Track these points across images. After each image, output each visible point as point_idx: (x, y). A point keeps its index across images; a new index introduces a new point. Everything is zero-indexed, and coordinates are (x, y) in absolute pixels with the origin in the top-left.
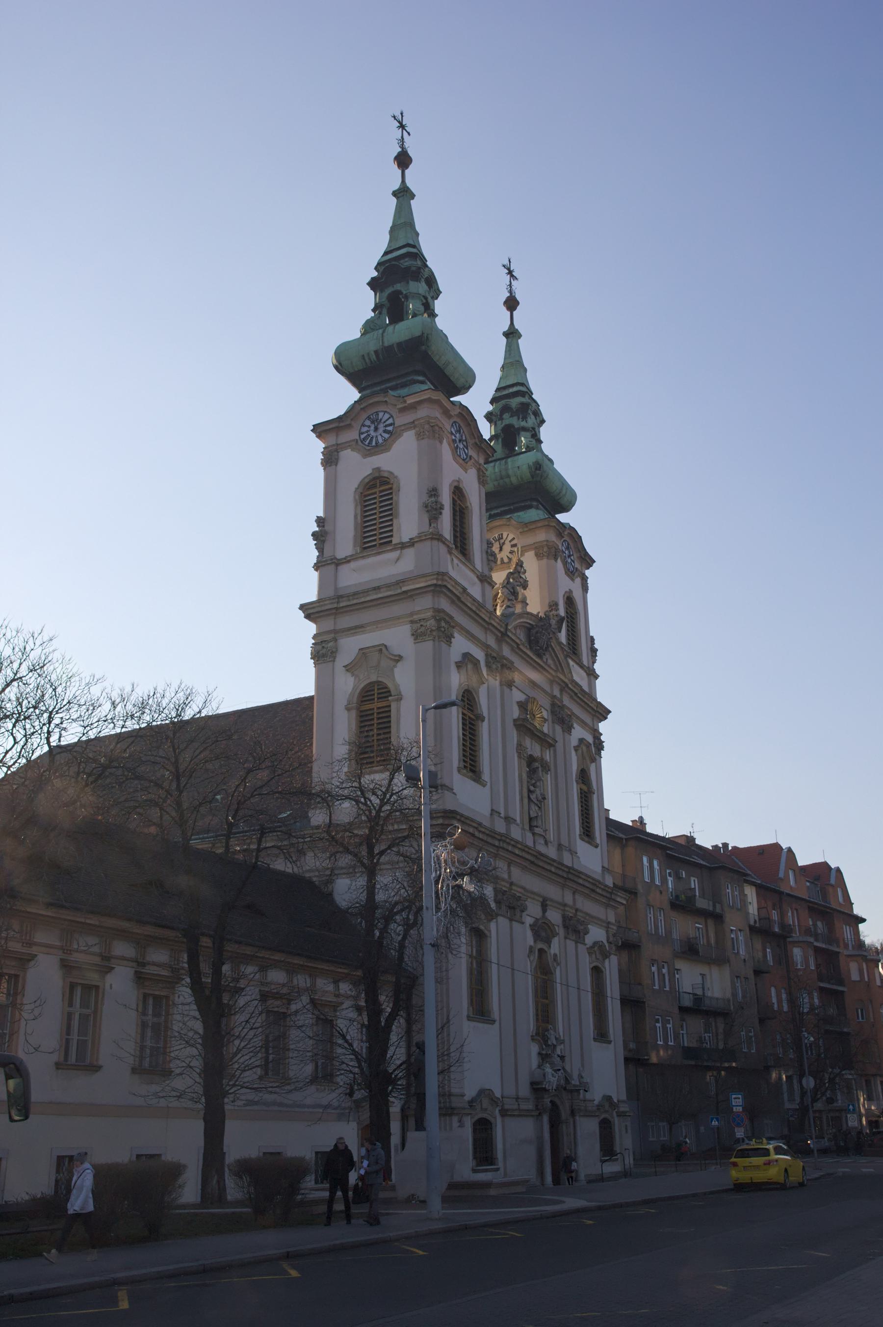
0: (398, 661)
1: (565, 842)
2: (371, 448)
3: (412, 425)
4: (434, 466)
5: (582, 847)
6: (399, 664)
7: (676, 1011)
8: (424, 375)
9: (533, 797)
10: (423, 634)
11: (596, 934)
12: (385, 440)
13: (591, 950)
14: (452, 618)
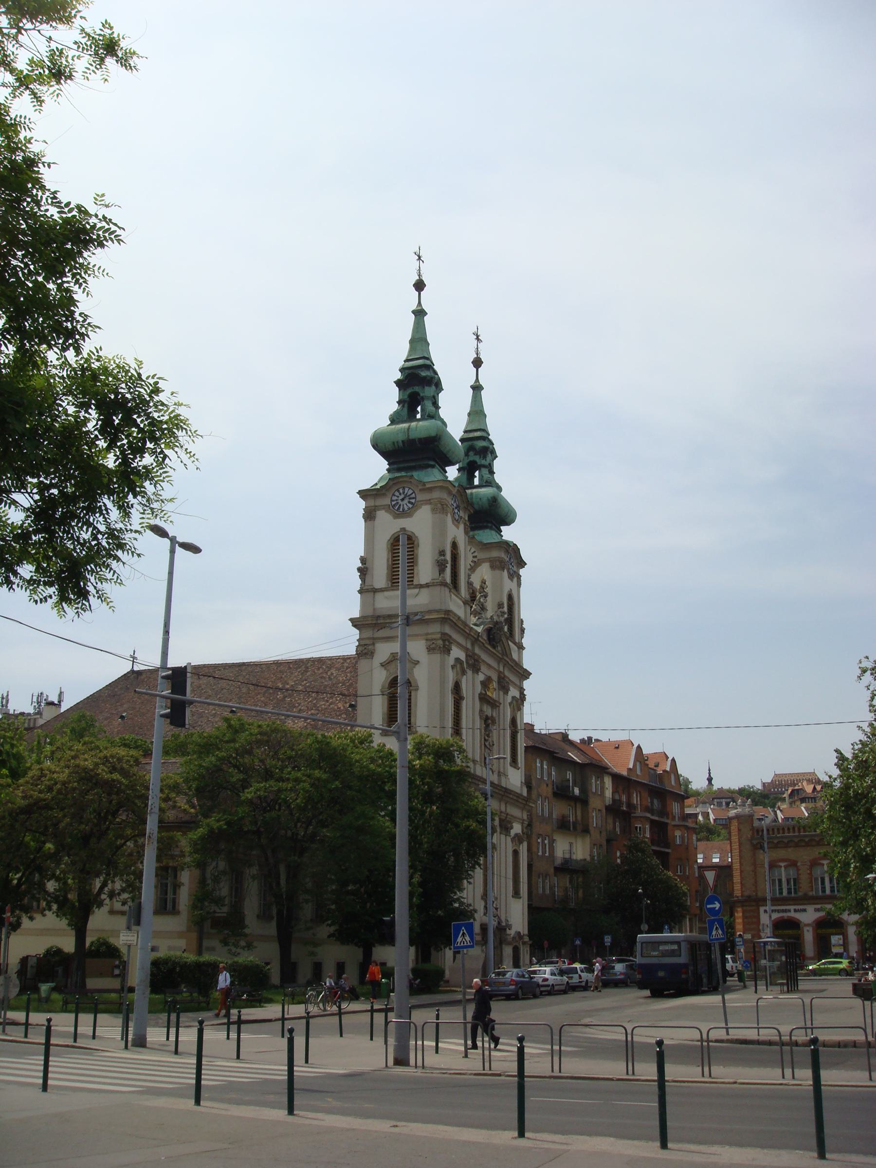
0: (416, 664)
1: (502, 770)
2: (400, 513)
3: (428, 502)
4: (440, 530)
5: (511, 771)
6: (417, 666)
7: (552, 870)
8: (434, 460)
9: (487, 744)
10: (434, 649)
11: (517, 828)
12: (409, 509)
13: (513, 840)
14: (450, 637)
